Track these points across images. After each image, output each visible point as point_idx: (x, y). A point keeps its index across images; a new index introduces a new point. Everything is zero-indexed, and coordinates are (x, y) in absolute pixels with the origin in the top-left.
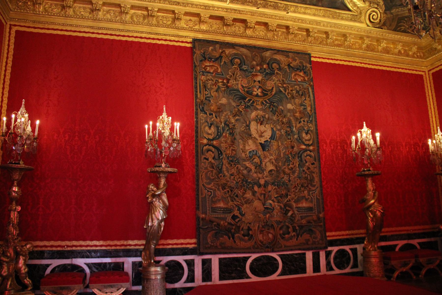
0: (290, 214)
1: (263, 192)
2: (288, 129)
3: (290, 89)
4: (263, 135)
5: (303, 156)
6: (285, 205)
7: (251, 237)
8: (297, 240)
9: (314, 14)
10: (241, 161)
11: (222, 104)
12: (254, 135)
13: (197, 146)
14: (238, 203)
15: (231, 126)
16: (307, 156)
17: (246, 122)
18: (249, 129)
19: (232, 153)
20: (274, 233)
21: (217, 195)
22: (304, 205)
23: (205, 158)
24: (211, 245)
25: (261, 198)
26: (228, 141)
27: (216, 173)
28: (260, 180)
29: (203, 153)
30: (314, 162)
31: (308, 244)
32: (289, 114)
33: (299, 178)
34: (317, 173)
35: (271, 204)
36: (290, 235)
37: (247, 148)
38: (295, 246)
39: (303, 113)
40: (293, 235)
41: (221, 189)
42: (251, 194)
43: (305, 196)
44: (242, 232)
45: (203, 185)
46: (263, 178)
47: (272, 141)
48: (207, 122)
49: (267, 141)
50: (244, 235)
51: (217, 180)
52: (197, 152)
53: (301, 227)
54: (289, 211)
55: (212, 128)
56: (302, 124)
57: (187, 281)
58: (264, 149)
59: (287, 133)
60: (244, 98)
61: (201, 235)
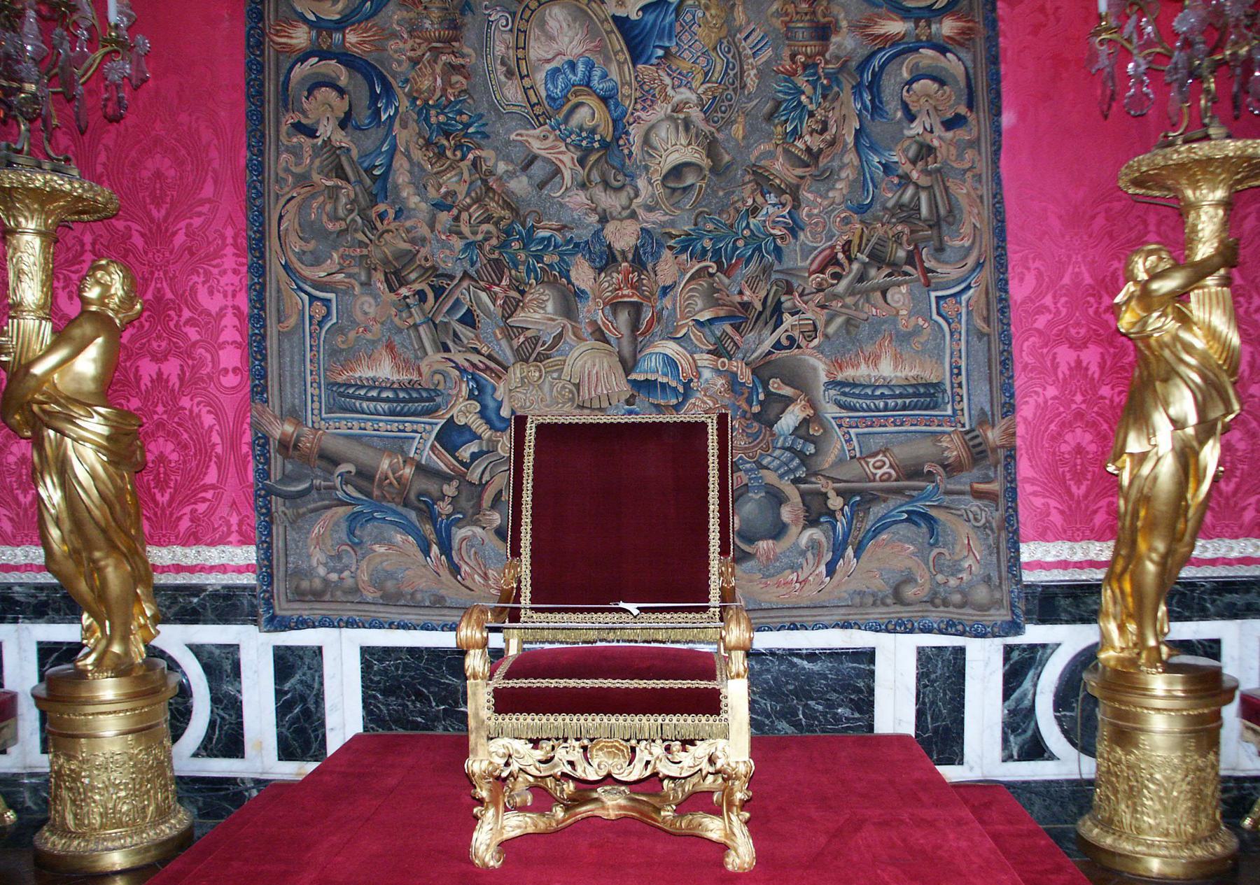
0: (789, 420)
5: (889, 86)
6: (762, 371)
8: (831, 571)
14: (475, 358)
16: (910, 83)
19: (447, 83)
21: (359, 316)
23: (299, 128)
24: (325, 581)
26: (427, 24)
28: (610, 227)
29: (285, 100)
30: (963, 110)
31: (899, 599)
33: (861, 209)
35: (671, 363)
36: (785, 543)
37: (537, 50)
40: (804, 539)
41: (382, 287)
42: (550, 307)
45: (286, 267)
46: (633, 215)
51: (360, 236)
52: (257, 96)
54: (787, 401)
57: (208, 748)
61: (277, 530)
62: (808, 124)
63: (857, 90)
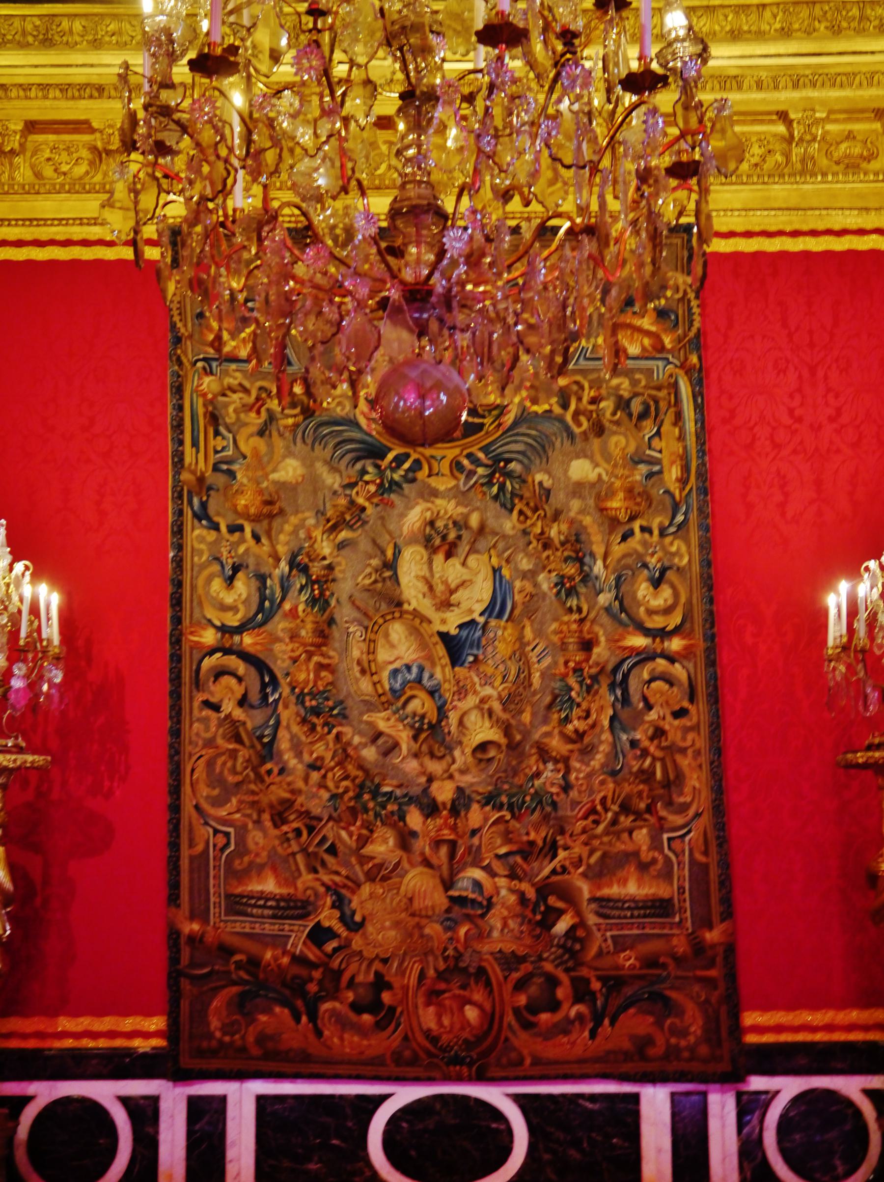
0: (562, 926)
1: (447, 834)
2: (570, 570)
3: (588, 394)
4: (454, 598)
5: (634, 684)
7: (386, 1018)
8: (593, 1034)
9: (732, 32)
10: (354, 714)
11: (282, 486)
12: (414, 604)
13: (177, 658)
14: (337, 879)
15: (316, 569)
16: (650, 682)
17: (383, 552)
18: (395, 579)
19: (317, 677)
20: (488, 1006)
21: (251, 845)
22: (633, 888)
23: (207, 704)
24: (220, 1042)
25: (435, 861)
26: (303, 633)
27: (248, 761)
28: (435, 786)
29: (197, 684)
30: (686, 704)
31: (643, 1057)
32: (575, 505)
33: (614, 774)
34: (698, 753)
35: (477, 884)
36: (559, 1016)
37: (383, 655)
38: (581, 1061)
39: (647, 496)
40: (573, 1013)
41: (268, 824)
42: (391, 842)
43: (636, 854)
44: (351, 996)
45: (197, 807)
46: (451, 777)
47: (493, 623)
48: (217, 559)
49: (473, 622)
50: (357, 1008)
51: (253, 787)
52: (176, 680)
53: (614, 982)
54: (560, 913)
55: (240, 584)
56: (635, 543)
58: (455, 659)
59: (566, 588)
60: (375, 452)
61: (185, 1005)
62: (576, 712)
63: (612, 687)
